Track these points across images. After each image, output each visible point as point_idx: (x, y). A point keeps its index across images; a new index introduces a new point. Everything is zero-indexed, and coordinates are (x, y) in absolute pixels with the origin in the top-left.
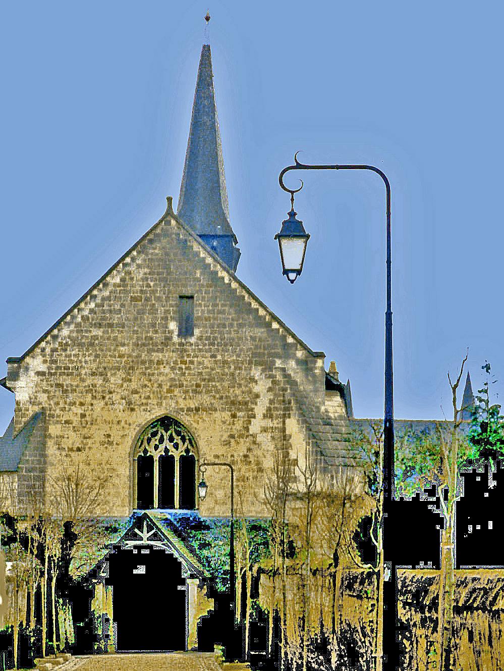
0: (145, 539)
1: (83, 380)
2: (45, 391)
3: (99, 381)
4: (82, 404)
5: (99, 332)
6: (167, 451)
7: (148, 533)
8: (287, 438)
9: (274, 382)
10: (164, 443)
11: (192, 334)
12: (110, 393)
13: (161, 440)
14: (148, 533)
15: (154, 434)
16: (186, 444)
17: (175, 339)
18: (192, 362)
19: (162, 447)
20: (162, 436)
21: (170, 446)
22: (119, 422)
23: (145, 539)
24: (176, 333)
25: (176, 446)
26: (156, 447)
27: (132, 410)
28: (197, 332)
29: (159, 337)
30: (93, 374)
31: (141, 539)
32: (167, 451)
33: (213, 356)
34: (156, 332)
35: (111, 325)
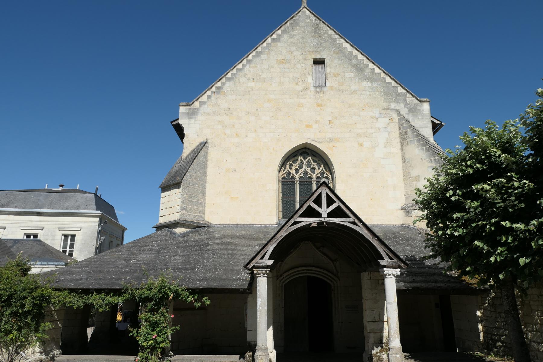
0: (324, 215)
6: (306, 173)
7: (328, 206)
8: (407, 161)
10: (303, 169)
12: (261, 128)
13: (301, 167)
14: (328, 207)
16: (321, 169)
17: (312, 89)
19: (301, 171)
20: (302, 162)
21: (308, 170)
23: (324, 215)
25: (313, 170)
26: (297, 171)
29: (300, 88)
30: (248, 114)
31: (319, 215)
32: (306, 173)
34: (297, 84)
35: (264, 81)
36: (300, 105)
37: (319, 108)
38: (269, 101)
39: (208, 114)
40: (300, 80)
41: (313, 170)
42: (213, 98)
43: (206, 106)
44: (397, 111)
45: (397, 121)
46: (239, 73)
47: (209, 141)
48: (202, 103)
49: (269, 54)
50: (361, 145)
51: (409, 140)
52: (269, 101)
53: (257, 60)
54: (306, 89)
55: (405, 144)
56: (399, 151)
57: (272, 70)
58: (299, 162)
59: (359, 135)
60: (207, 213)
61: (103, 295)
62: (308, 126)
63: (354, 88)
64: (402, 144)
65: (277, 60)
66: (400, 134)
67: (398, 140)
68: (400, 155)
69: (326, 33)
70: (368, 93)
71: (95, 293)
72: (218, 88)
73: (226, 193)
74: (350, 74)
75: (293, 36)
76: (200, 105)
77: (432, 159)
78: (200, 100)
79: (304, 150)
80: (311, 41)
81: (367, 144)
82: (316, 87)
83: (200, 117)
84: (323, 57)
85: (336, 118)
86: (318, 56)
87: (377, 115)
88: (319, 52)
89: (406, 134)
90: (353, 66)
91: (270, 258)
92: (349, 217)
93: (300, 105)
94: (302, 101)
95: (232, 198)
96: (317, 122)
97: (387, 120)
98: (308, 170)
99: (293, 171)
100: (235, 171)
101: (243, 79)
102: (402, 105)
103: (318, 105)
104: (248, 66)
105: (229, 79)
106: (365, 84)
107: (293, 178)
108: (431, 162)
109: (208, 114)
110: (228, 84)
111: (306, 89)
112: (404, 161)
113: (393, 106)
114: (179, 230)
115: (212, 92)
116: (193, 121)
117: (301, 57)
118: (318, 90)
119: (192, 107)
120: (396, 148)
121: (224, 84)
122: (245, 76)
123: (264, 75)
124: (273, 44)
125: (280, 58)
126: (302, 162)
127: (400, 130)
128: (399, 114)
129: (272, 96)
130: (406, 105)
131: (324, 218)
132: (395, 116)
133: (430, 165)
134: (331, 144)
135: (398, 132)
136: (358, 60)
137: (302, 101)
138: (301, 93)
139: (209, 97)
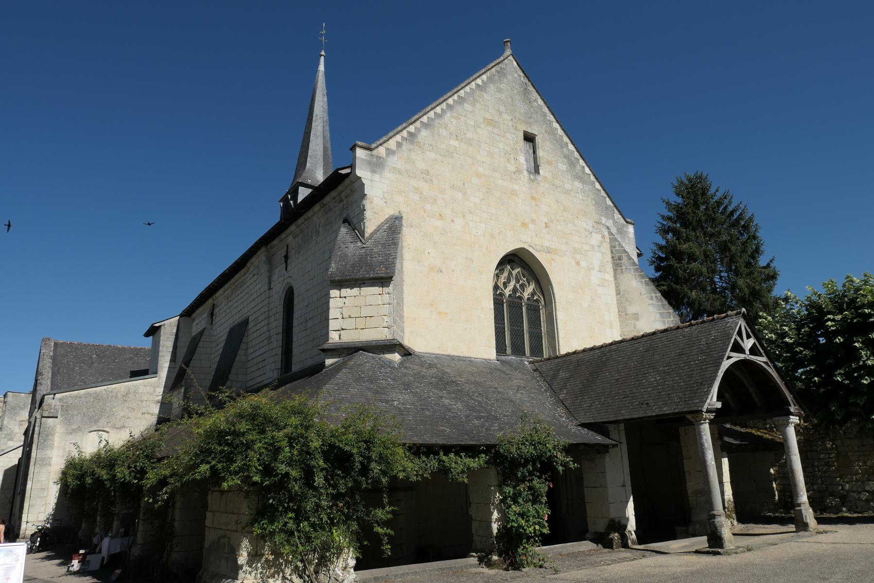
5: (455, 143)
9: (603, 237)
12: (471, 213)
17: (526, 173)
29: (512, 168)
30: (453, 187)
32: (515, 290)
35: (469, 142)
36: (514, 193)
37: (533, 203)
38: (478, 175)
39: (399, 172)
40: (512, 156)
41: (523, 286)
42: (404, 148)
43: (395, 158)
46: (437, 121)
48: (390, 152)
50: (578, 263)
51: (624, 267)
52: (478, 175)
53: (459, 108)
55: (619, 271)
56: (613, 279)
57: (479, 130)
58: (506, 274)
59: (575, 251)
60: (407, 330)
61: (452, 455)
63: (568, 186)
64: (615, 271)
65: (485, 119)
66: (613, 258)
67: (611, 265)
68: (613, 285)
69: (536, 101)
71: (442, 453)
73: (431, 305)
74: (563, 166)
75: (500, 90)
76: (387, 155)
77: (653, 295)
78: (385, 145)
79: (510, 258)
80: (521, 107)
81: (583, 264)
82: (530, 172)
83: (388, 174)
84: (534, 132)
85: (552, 221)
86: (530, 130)
87: (591, 229)
89: (620, 259)
91: (718, 400)
92: (761, 355)
94: (516, 187)
95: (440, 313)
96: (533, 221)
97: (599, 237)
98: (518, 286)
100: (441, 271)
101: (443, 132)
102: (611, 221)
103: (533, 198)
104: (449, 114)
105: (425, 126)
106: (577, 184)
108: (652, 299)
110: (424, 133)
111: (518, 171)
112: (618, 293)
114: (396, 357)
116: (377, 177)
117: (510, 124)
119: (374, 152)
120: (609, 276)
121: (418, 130)
122: (445, 128)
123: (469, 135)
124: (478, 93)
126: (510, 273)
127: (612, 252)
128: (610, 233)
130: (615, 222)
131: (747, 356)
133: (651, 302)
134: (549, 255)
135: (609, 255)
136: (569, 150)
139: (399, 145)
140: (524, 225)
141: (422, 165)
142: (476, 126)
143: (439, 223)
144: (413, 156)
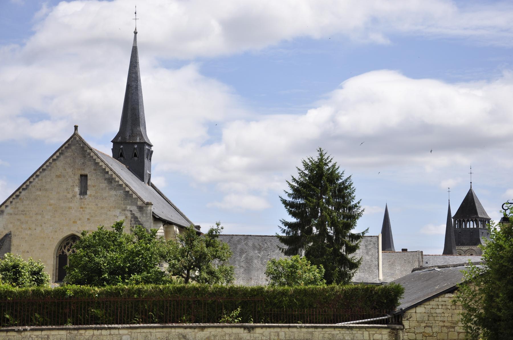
1: (31, 217)
2: (11, 223)
3: (39, 217)
4: (30, 229)
9: (126, 217)
11: (86, 194)
15: (67, 244)
17: (78, 196)
18: (85, 208)
19: (71, 250)
22: (49, 238)
24: (78, 193)
26: (68, 250)
27: (56, 232)
28: (88, 193)
29: (70, 196)
30: (37, 214)
33: (97, 205)
34: (68, 193)
35: (46, 190)
36: (70, 208)
37: (82, 210)
38: (50, 205)
42: (14, 203)
44: (131, 211)
45: (130, 218)
47: (12, 233)
48: (6, 206)
49: (50, 170)
52: (50, 205)
54: (74, 196)
62: (75, 222)
65: (56, 175)
70: (114, 199)
72: (17, 196)
74: (104, 184)
85: (92, 216)
86: (83, 173)
88: (84, 169)
90: (105, 179)
93: (70, 208)
94: (71, 205)
96: (80, 219)
99: (66, 251)
103: (81, 208)
104: (37, 180)
107: (66, 255)
109: (11, 214)
113: (128, 207)
115: (13, 199)
118: (82, 197)
121: (20, 192)
125: (58, 173)
128: (131, 214)
129: (52, 202)
132: (129, 214)
137: (71, 205)
138: (70, 200)
140: (75, 222)
141: (21, 208)
142: (52, 180)
143: (29, 232)
144: (18, 205)
